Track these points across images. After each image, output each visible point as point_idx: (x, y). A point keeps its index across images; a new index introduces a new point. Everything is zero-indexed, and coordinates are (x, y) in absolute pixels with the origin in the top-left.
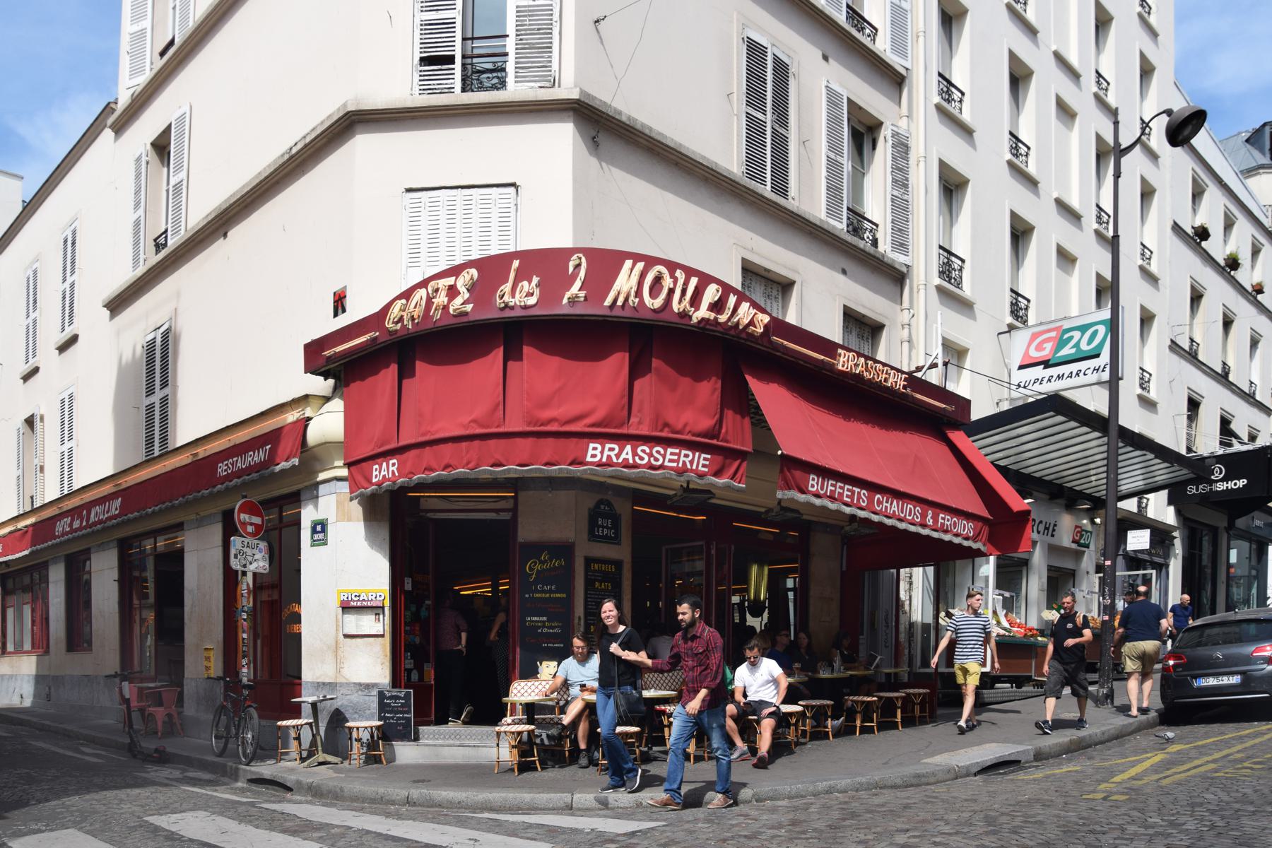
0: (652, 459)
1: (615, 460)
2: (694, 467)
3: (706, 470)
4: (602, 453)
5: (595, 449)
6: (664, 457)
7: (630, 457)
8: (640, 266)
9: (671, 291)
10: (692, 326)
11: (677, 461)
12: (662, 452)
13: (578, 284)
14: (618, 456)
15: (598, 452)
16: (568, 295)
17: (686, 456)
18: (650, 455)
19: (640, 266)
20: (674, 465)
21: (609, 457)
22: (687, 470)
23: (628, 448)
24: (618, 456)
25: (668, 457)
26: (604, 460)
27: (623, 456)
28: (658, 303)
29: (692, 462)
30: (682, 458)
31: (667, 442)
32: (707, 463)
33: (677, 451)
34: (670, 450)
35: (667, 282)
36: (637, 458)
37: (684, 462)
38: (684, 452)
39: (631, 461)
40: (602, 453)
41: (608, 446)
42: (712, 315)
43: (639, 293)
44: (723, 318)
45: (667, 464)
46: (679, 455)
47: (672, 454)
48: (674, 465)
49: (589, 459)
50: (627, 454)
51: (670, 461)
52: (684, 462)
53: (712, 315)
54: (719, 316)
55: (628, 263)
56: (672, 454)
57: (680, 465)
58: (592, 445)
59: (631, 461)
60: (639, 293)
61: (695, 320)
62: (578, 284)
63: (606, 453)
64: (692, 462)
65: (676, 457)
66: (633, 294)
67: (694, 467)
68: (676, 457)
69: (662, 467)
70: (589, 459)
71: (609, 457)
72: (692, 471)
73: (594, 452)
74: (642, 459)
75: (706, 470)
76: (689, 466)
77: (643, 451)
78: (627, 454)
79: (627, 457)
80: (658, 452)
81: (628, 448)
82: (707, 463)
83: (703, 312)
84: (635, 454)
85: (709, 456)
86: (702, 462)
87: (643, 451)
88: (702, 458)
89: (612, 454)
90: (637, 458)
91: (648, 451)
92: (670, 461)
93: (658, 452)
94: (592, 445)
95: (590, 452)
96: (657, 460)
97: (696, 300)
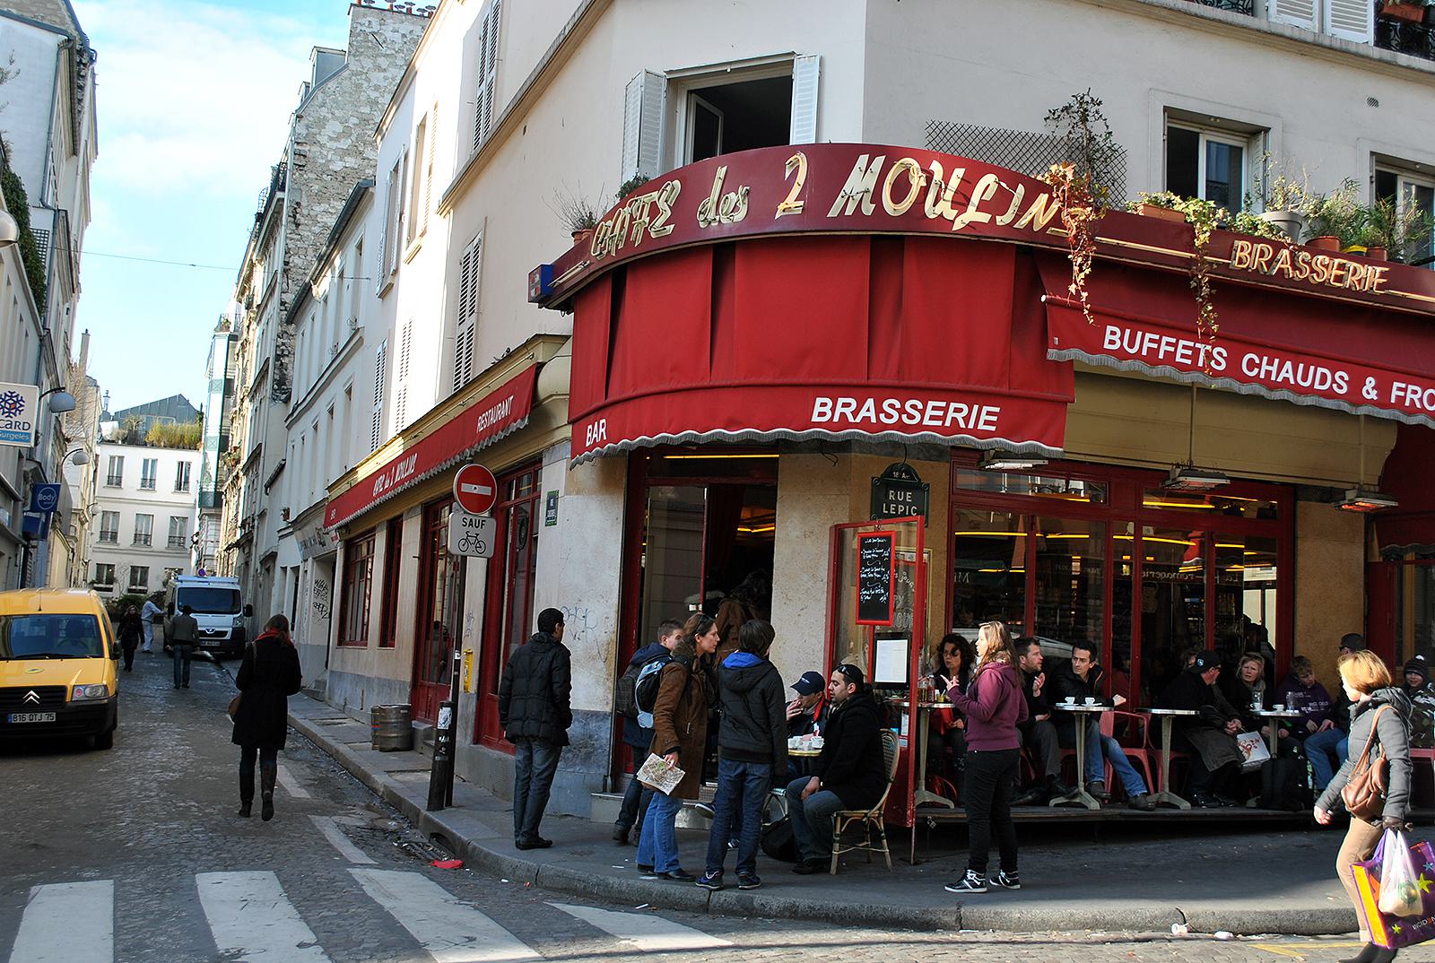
0: (904, 417)
1: (851, 419)
2: (971, 426)
3: (993, 428)
4: (833, 410)
5: (824, 405)
6: (922, 412)
7: (872, 415)
8: (880, 160)
9: (924, 191)
10: (956, 233)
11: (943, 418)
12: (920, 406)
13: (796, 190)
14: (855, 414)
15: (827, 409)
16: (782, 206)
17: (957, 410)
18: (902, 411)
19: (880, 160)
20: (940, 423)
21: (843, 415)
22: (961, 431)
23: (870, 403)
24: (855, 414)
25: (929, 412)
26: (836, 419)
27: (863, 413)
28: (906, 205)
29: (967, 419)
30: (951, 414)
31: (926, 393)
32: (994, 419)
33: (943, 404)
34: (931, 404)
35: (917, 181)
36: (882, 416)
37: (954, 419)
38: (953, 405)
39: (874, 420)
40: (833, 410)
41: (841, 401)
42: (984, 218)
43: (877, 197)
44: (1002, 220)
45: (926, 422)
46: (946, 410)
47: (934, 408)
48: (940, 423)
49: (815, 418)
50: (868, 410)
51: (932, 418)
52: (954, 419)
53: (984, 218)
54: (998, 218)
55: (864, 159)
56: (934, 408)
57: (948, 424)
58: (819, 400)
59: (874, 420)
60: (877, 197)
61: (957, 226)
62: (796, 190)
63: (839, 409)
64: (967, 419)
65: (940, 413)
66: (868, 197)
67: (971, 426)
68: (940, 413)
69: (920, 427)
70: (815, 418)
71: (843, 415)
72: (967, 431)
73: (823, 409)
74: (889, 416)
75: (993, 428)
76: (962, 425)
77: (892, 406)
78: (868, 410)
79: (868, 414)
80: (914, 407)
81: (870, 403)
82: (994, 419)
83: (972, 215)
84: (879, 410)
85: (997, 410)
86: (984, 417)
87: (892, 406)
88: (984, 412)
89: (848, 411)
90: (882, 416)
91: (898, 405)
92: (932, 418)
93: (914, 407)
94: (819, 400)
95: (818, 409)
96: (911, 417)
97: (961, 202)
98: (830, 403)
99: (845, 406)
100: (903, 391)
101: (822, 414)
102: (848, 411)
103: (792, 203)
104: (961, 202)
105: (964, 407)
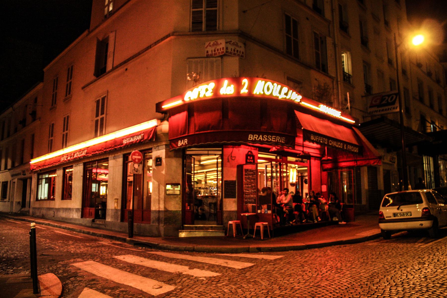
1: (257, 139)
4: (253, 137)
5: (251, 136)
6: (271, 138)
7: (261, 139)
14: (258, 138)
15: (252, 137)
18: (267, 138)
20: (274, 141)
21: (255, 139)
23: (261, 136)
24: (258, 138)
26: (254, 139)
27: (259, 138)
31: (272, 134)
34: (273, 136)
37: (277, 140)
38: (277, 137)
41: (255, 135)
42: (285, 96)
45: (272, 141)
46: (276, 138)
48: (274, 141)
49: (249, 139)
52: (277, 140)
58: (250, 135)
59: (262, 140)
63: (254, 137)
70: (249, 139)
71: (255, 139)
77: (265, 137)
80: (270, 137)
81: (261, 136)
84: (263, 138)
87: (265, 137)
89: (256, 138)
92: (273, 140)
93: (270, 137)
94: (250, 135)
95: (249, 137)
97: (280, 93)
98: (252, 136)
100: (268, 134)
101: (250, 138)
102: (256, 138)
104: (280, 93)
105: (279, 137)
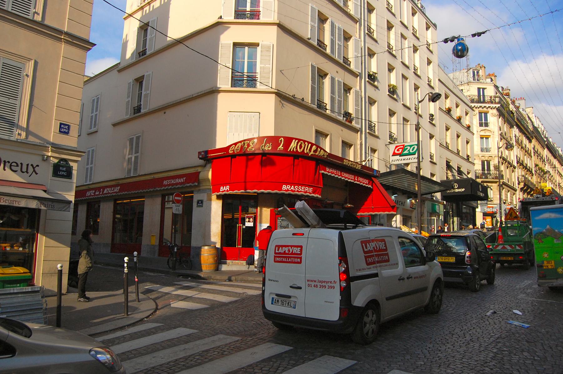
4: (286, 188)
5: (284, 186)
6: (301, 189)
8: (297, 141)
11: (305, 190)
13: (282, 145)
14: (290, 188)
15: (285, 187)
16: (279, 148)
18: (298, 188)
19: (297, 141)
21: (288, 189)
23: (293, 186)
24: (290, 188)
25: (302, 189)
27: (291, 188)
28: (302, 150)
29: (308, 190)
35: (303, 146)
40: (286, 188)
41: (288, 186)
46: (305, 188)
49: (283, 189)
51: (303, 190)
55: (294, 140)
58: (284, 186)
62: (282, 145)
63: (287, 188)
64: (308, 190)
81: (293, 186)
83: (312, 153)
84: (294, 188)
86: (311, 190)
92: (303, 190)
94: (284, 186)
99: (288, 187)
101: (284, 188)
102: (289, 188)
103: (281, 147)
104: (310, 150)
